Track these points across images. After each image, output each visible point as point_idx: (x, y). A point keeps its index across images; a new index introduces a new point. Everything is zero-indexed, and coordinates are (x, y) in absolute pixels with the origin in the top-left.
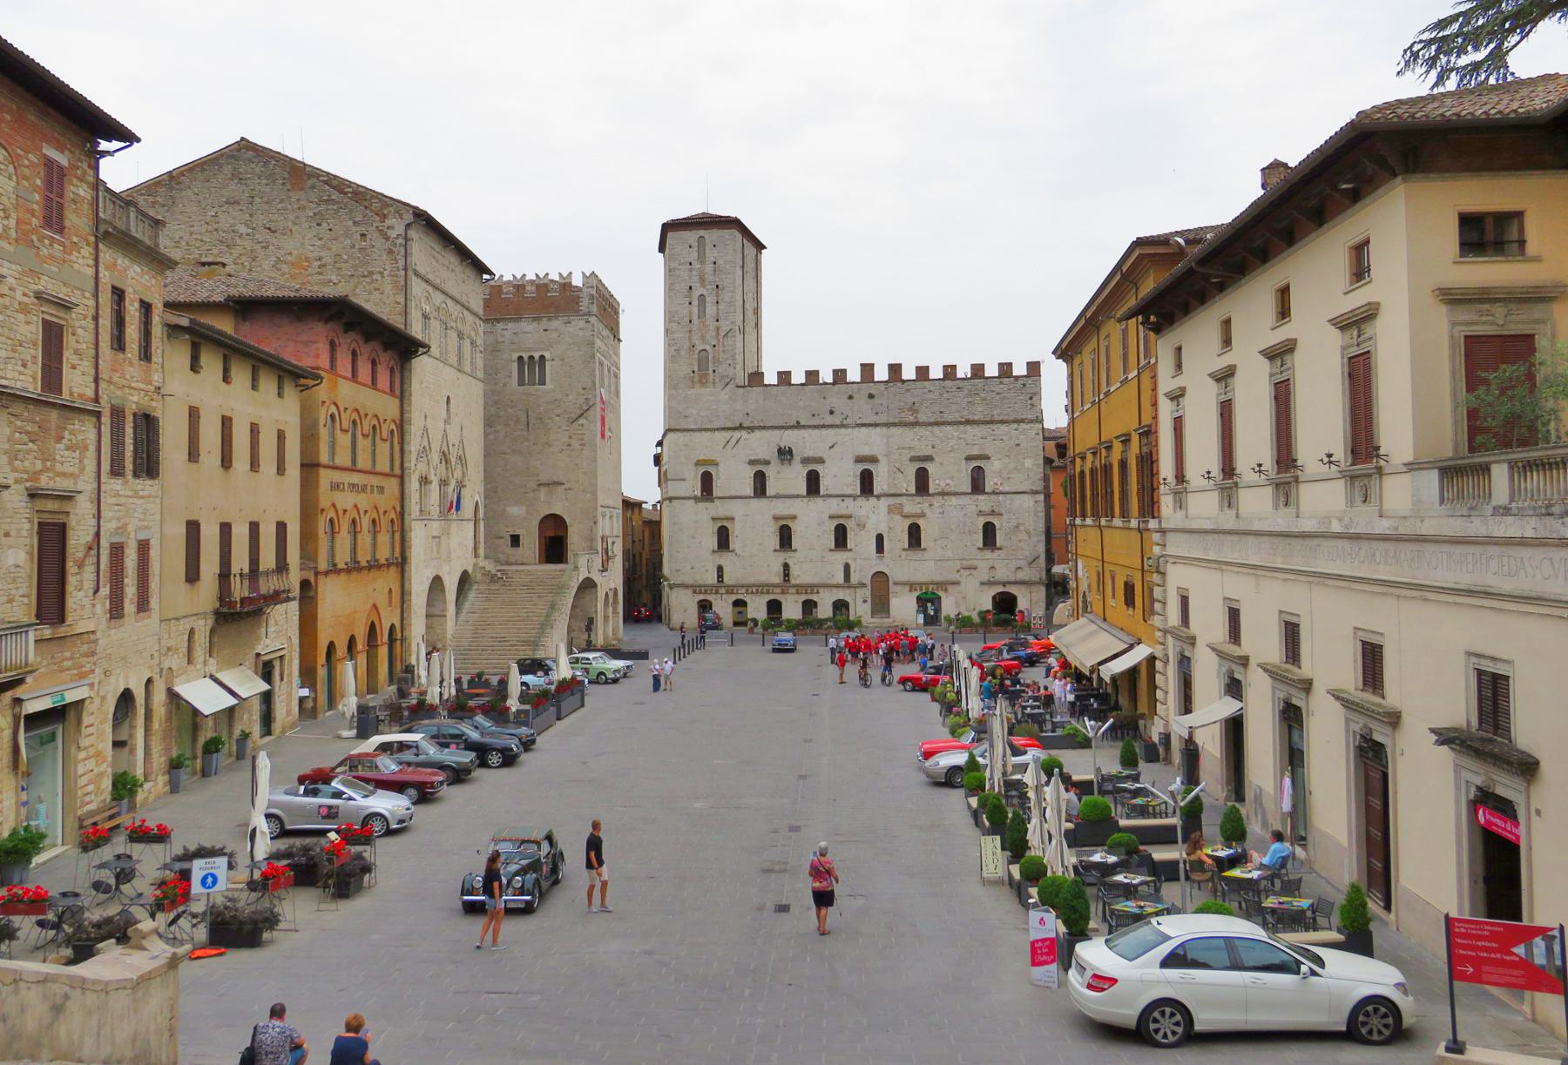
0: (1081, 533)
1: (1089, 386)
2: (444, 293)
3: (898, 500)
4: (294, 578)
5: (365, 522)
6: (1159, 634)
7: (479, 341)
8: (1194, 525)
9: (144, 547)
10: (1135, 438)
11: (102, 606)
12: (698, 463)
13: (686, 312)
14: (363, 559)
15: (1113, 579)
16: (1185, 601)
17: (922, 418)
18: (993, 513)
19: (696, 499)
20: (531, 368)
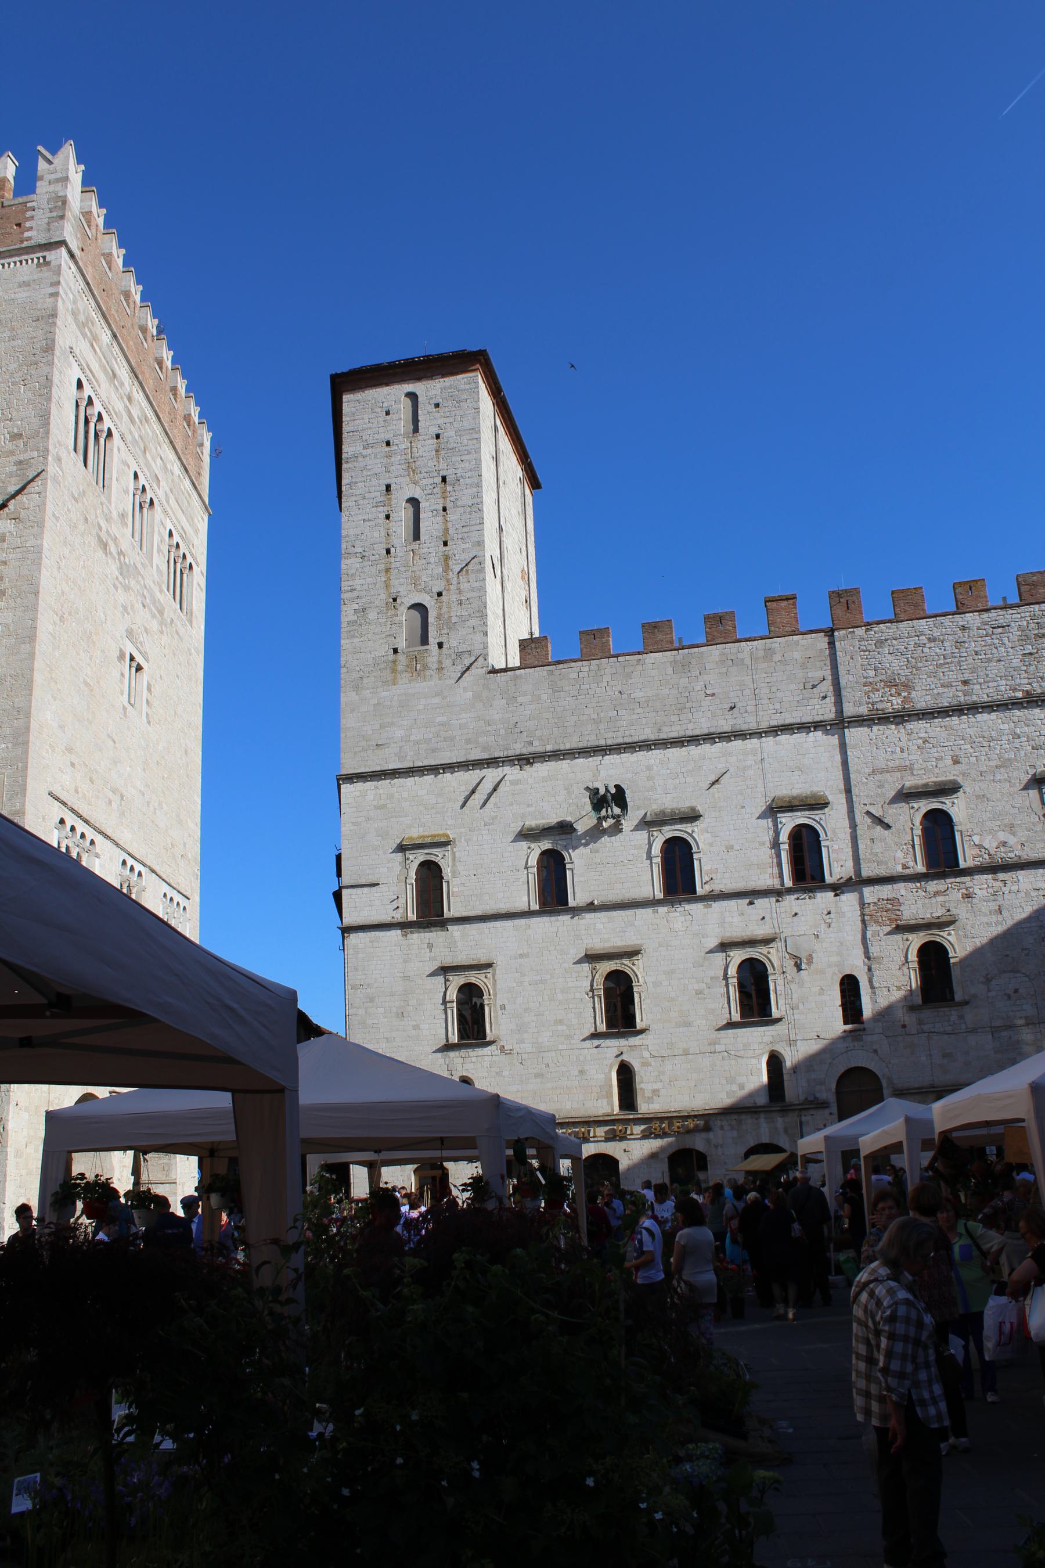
13: (378, 534)
17: (921, 700)
19: (405, 926)
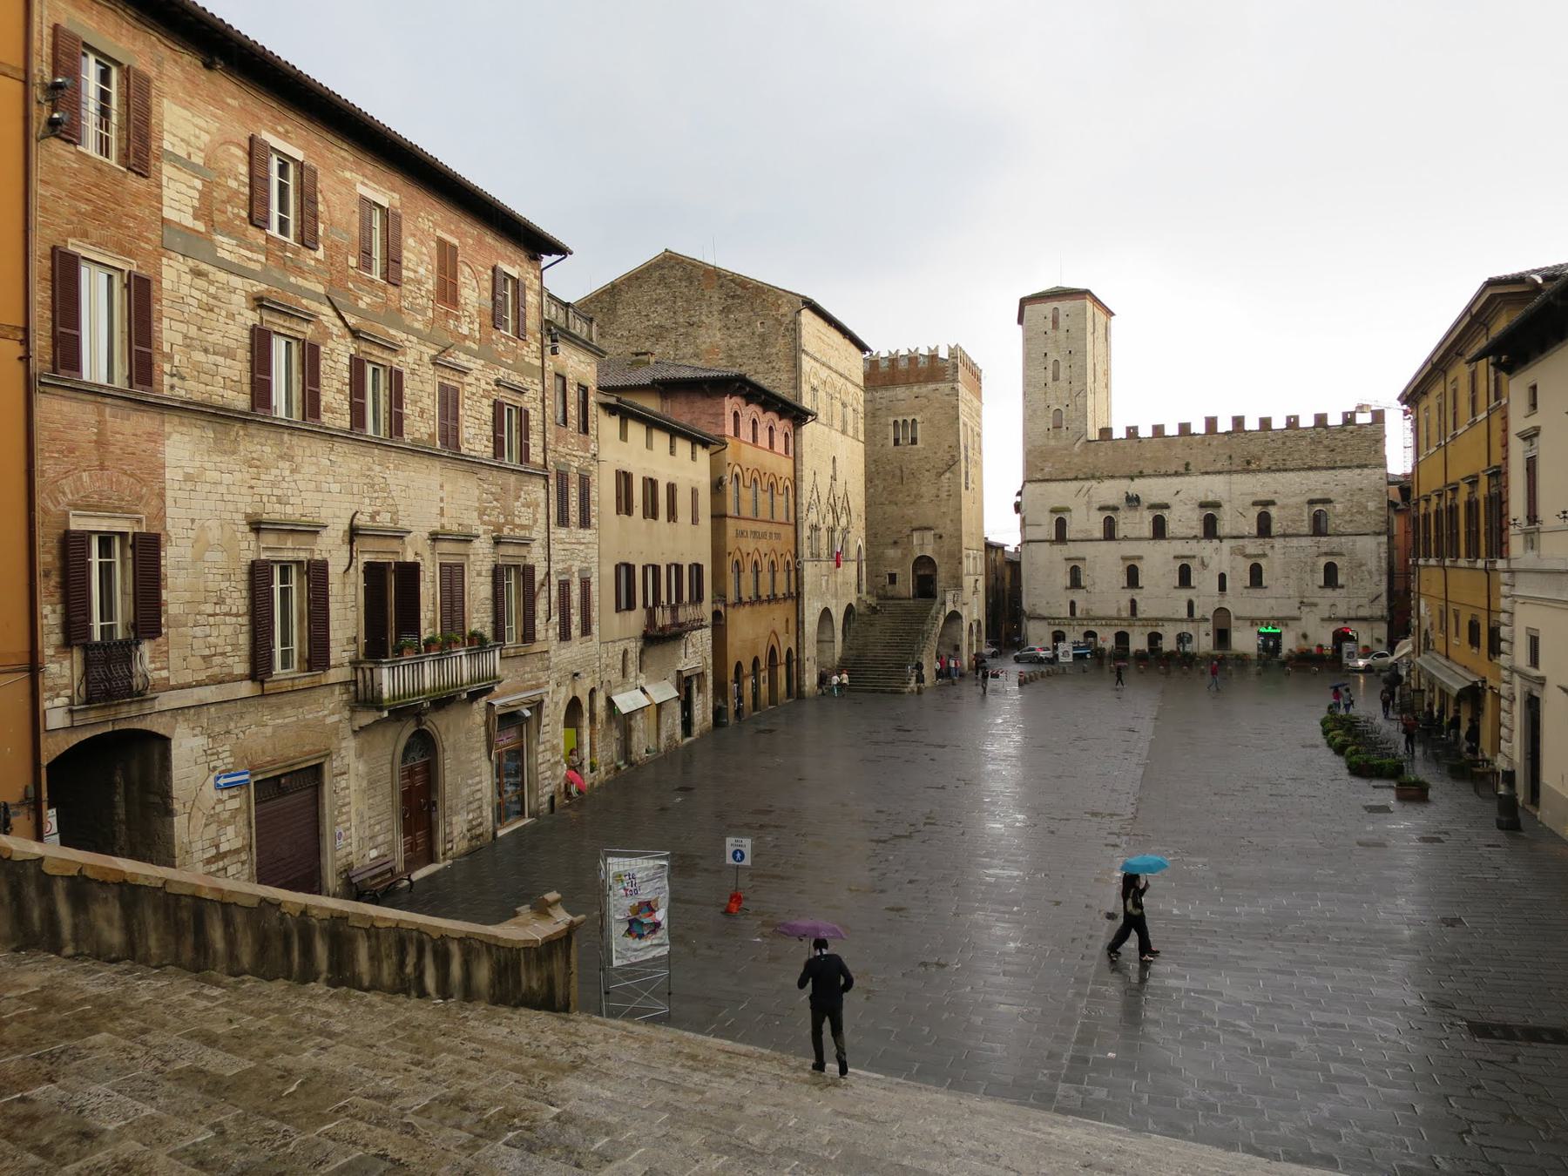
0: (1424, 573)
1: (1434, 429)
2: (830, 368)
3: (1240, 542)
4: (706, 609)
5: (765, 564)
6: (1504, 673)
7: (861, 409)
8: (1547, 566)
9: (585, 584)
10: (1484, 480)
11: (553, 633)
12: (1053, 511)
14: (765, 591)
15: (1457, 617)
16: (1534, 642)
18: (1332, 554)
20: (905, 432)
